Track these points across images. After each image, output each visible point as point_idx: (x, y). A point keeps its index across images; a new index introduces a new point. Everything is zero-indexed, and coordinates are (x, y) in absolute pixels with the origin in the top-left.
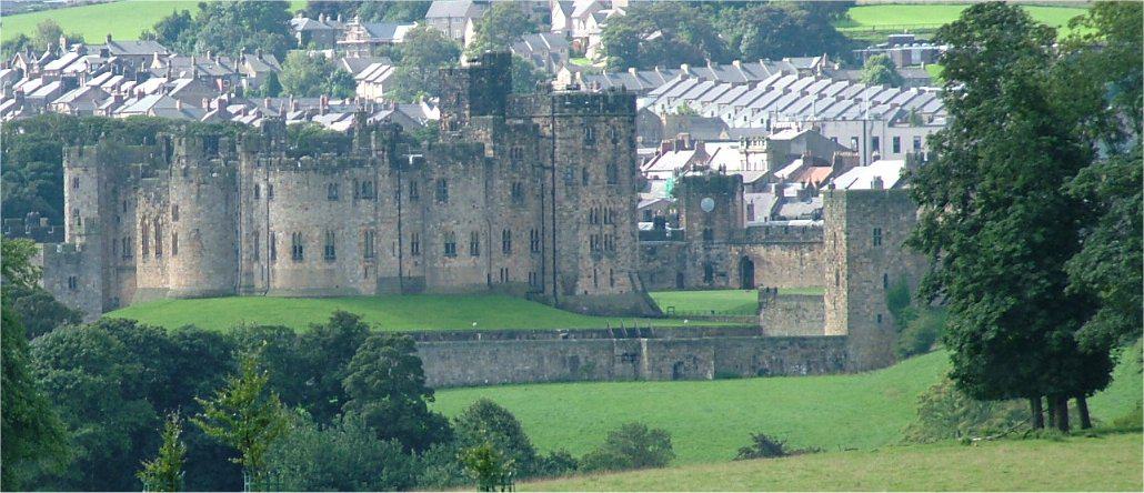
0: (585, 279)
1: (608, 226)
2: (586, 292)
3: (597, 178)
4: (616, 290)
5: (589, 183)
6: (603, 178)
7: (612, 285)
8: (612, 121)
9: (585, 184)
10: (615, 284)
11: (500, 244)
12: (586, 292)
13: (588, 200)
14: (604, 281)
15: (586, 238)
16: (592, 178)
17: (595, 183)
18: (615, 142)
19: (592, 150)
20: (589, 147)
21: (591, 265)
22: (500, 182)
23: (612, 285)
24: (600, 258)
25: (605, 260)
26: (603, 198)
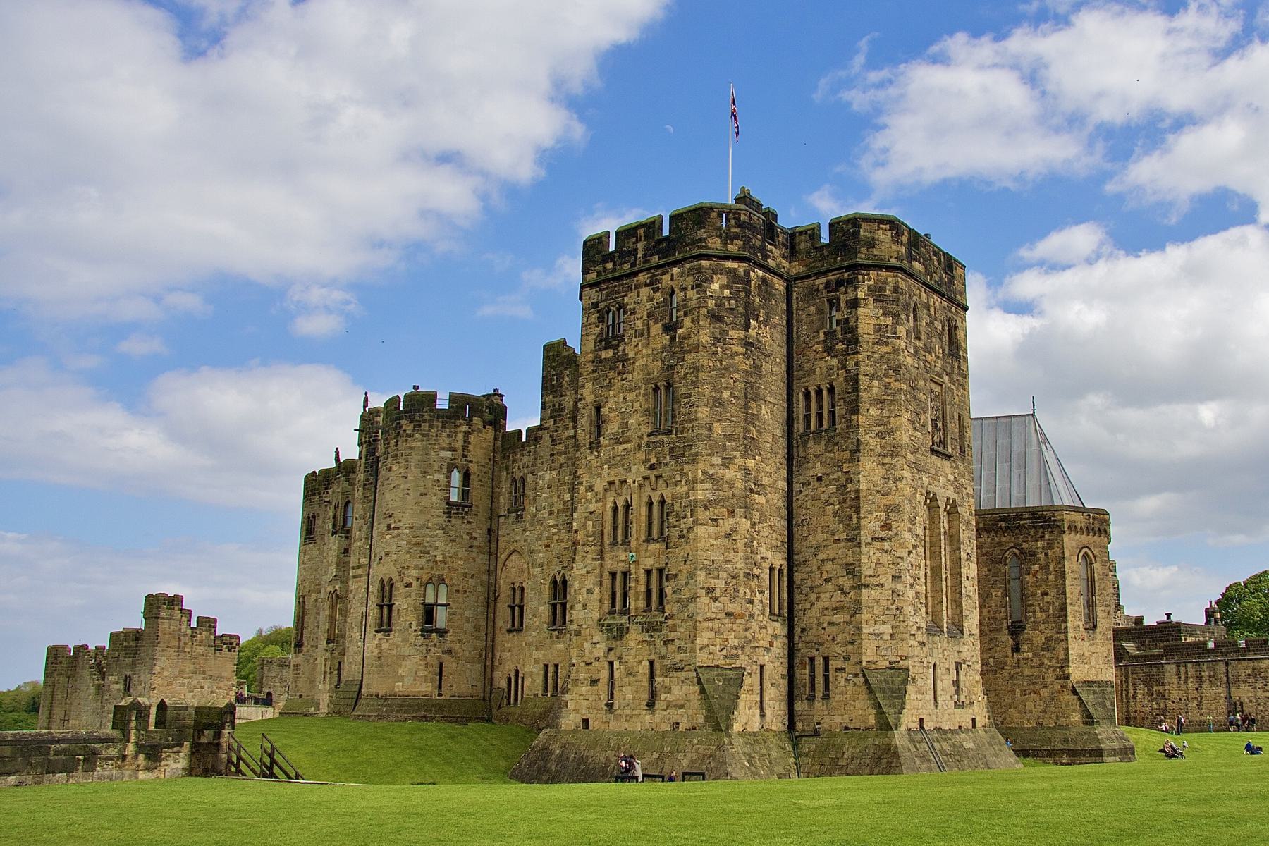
0: (586, 689)
1: (654, 547)
2: (586, 722)
3: (624, 425)
4: (661, 719)
5: (604, 441)
6: (639, 425)
7: (651, 705)
8: (666, 279)
9: (595, 445)
10: (660, 705)
11: (545, 611)
12: (586, 722)
13: (600, 485)
14: (630, 693)
15: (590, 582)
16: (612, 427)
17: (618, 442)
18: (670, 328)
19: (616, 359)
20: (609, 354)
21: (600, 651)
22: (548, 476)
23: (651, 705)
24: (622, 631)
25: (634, 636)
26: (637, 472)
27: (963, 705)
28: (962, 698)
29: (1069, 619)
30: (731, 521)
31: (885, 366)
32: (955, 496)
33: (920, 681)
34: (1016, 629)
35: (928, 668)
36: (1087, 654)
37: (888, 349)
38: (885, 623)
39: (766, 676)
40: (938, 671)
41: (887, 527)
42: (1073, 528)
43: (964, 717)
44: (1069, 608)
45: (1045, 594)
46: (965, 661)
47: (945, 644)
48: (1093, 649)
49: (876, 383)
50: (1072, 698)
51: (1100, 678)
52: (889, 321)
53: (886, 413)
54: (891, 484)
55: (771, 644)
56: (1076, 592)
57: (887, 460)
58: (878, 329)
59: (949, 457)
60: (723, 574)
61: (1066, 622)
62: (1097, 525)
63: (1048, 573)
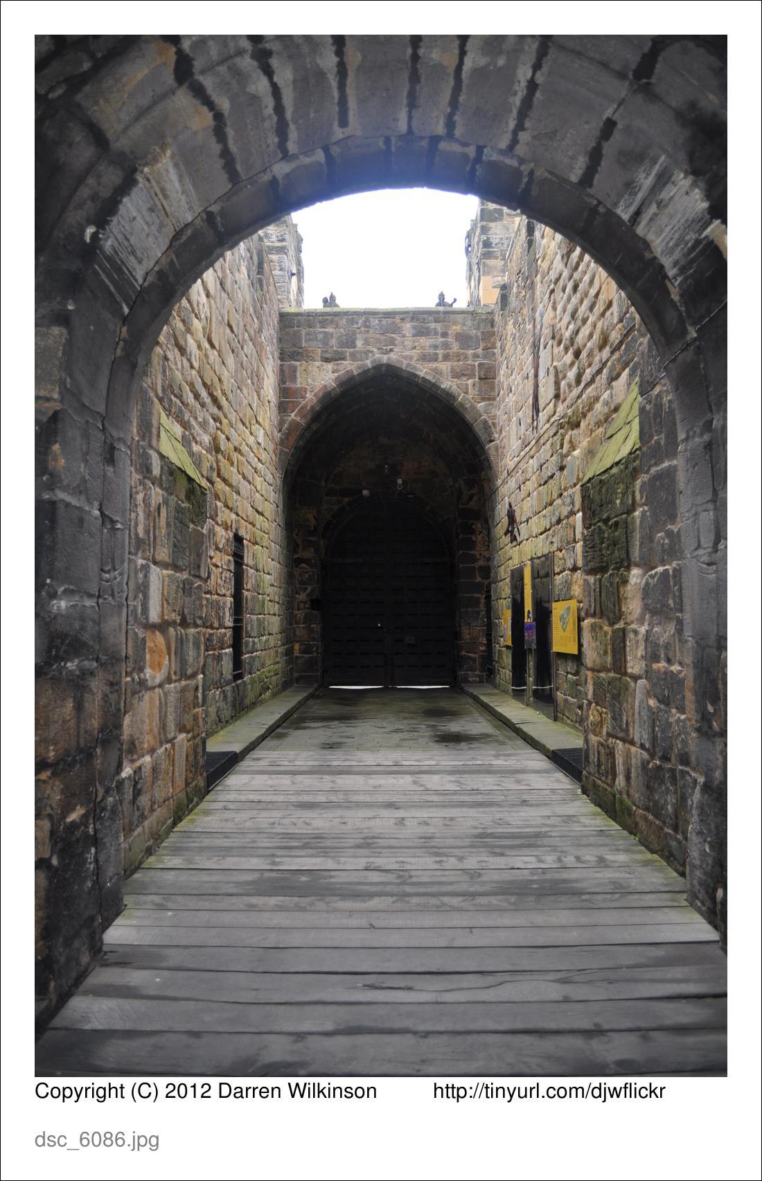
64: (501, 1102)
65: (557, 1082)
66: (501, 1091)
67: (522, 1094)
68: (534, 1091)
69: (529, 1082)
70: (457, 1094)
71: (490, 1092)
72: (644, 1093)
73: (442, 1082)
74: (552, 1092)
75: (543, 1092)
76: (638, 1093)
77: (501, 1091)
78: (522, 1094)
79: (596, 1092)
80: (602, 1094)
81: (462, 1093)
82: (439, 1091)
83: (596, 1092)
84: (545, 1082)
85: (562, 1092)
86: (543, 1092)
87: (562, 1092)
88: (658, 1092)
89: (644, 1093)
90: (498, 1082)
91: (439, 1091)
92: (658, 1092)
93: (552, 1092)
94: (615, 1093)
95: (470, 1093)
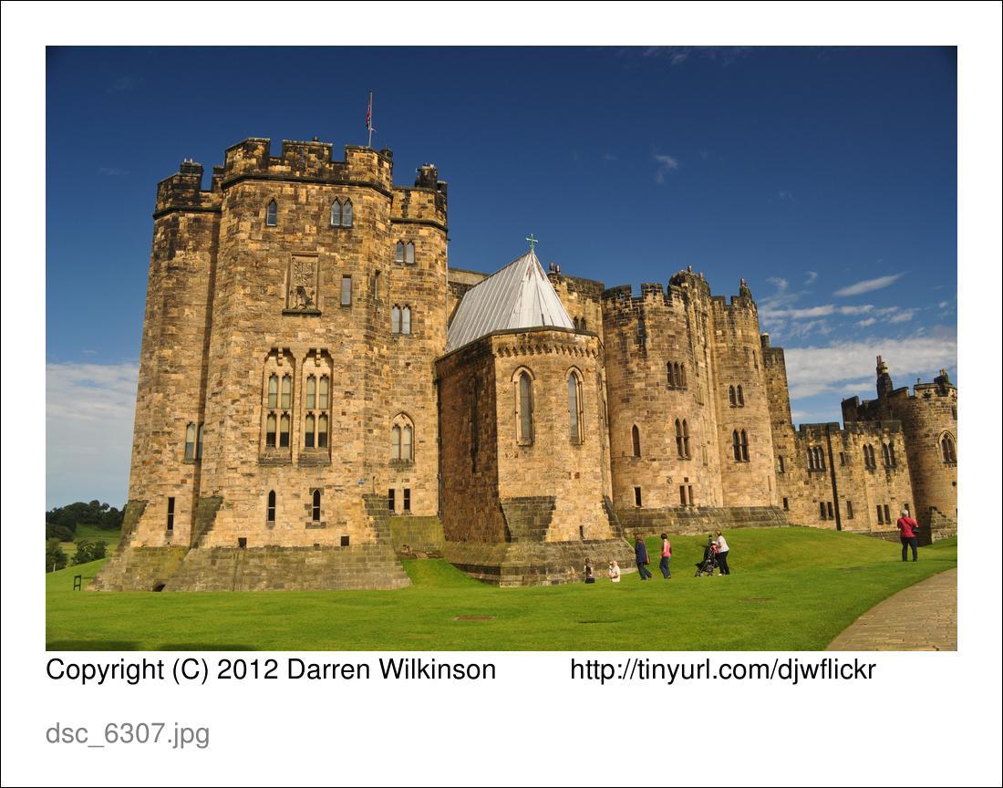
27: (323, 525)
28: (322, 519)
29: (499, 438)
30: (149, 396)
31: (230, 257)
32: (329, 346)
33: (241, 507)
34: (474, 452)
35: (258, 495)
36: (521, 471)
37: (233, 243)
38: (213, 460)
39: (176, 505)
40: (278, 498)
41: (220, 383)
42: (503, 350)
43: (331, 537)
44: (500, 428)
45: (487, 416)
46: (329, 487)
47: (293, 473)
48: (528, 465)
49: (224, 273)
50: (500, 515)
51: (537, 493)
52: (235, 221)
53: (227, 294)
54: (225, 350)
55: (184, 482)
56: (509, 412)
57: (224, 330)
58: (229, 230)
59: (318, 314)
60: (143, 434)
61: (496, 441)
62: (533, 342)
63: (488, 397)
64: (659, 683)
65: (733, 657)
66: (659, 669)
67: (688, 673)
68: (703, 670)
69: (697, 657)
70: (602, 674)
71: (646, 672)
72: (847, 672)
73: (582, 657)
74: (726, 672)
75: (714, 670)
76: (839, 672)
77: (659, 669)
78: (688, 673)
79: (785, 671)
80: (792, 673)
81: (608, 672)
82: (578, 669)
83: (785, 671)
84: (718, 658)
85: (740, 672)
86: (714, 670)
87: (740, 672)
88: (866, 670)
89: (847, 672)
90: (655, 657)
91: (578, 669)
92: (866, 670)
93: (726, 672)
94: (810, 672)
95: (619, 672)
